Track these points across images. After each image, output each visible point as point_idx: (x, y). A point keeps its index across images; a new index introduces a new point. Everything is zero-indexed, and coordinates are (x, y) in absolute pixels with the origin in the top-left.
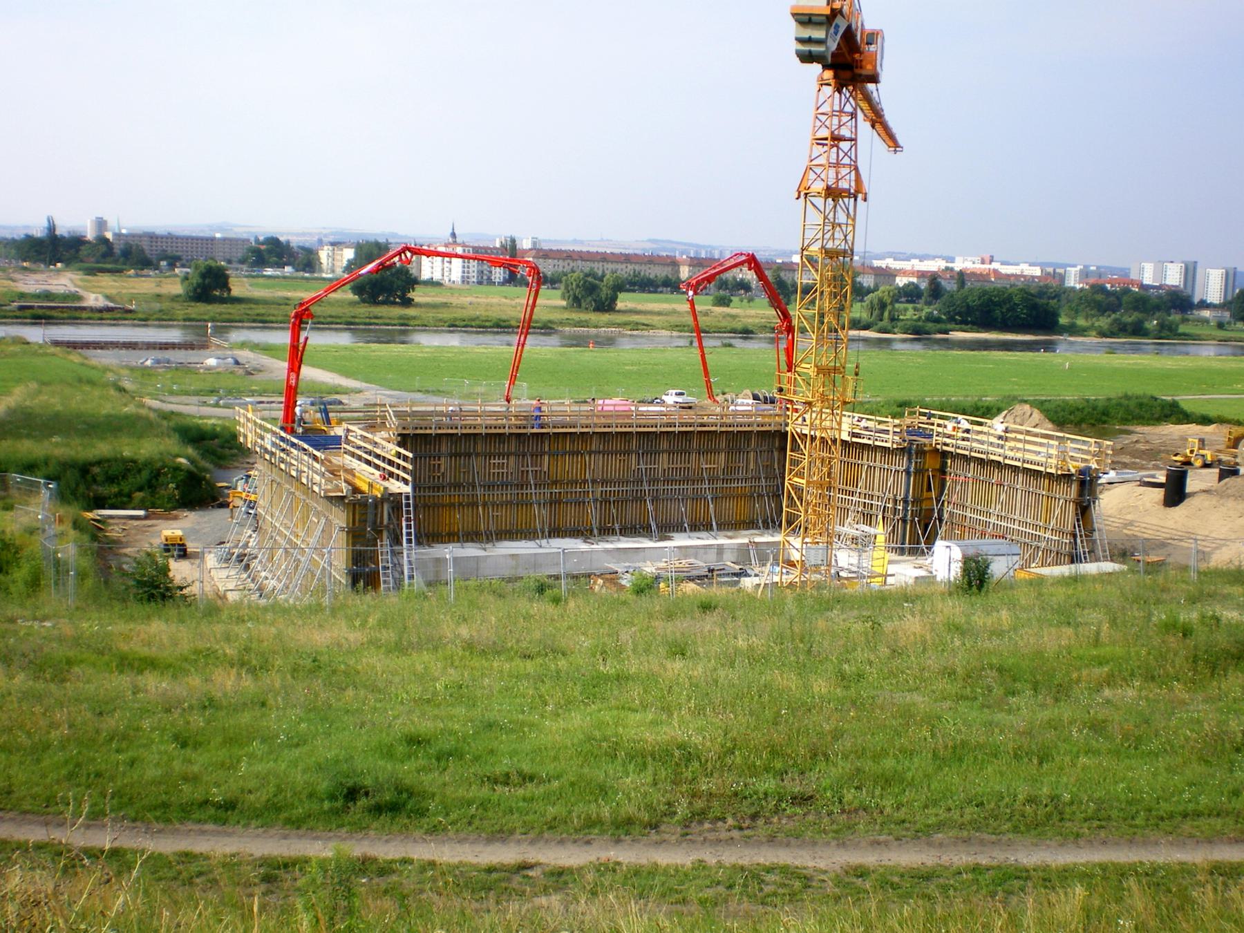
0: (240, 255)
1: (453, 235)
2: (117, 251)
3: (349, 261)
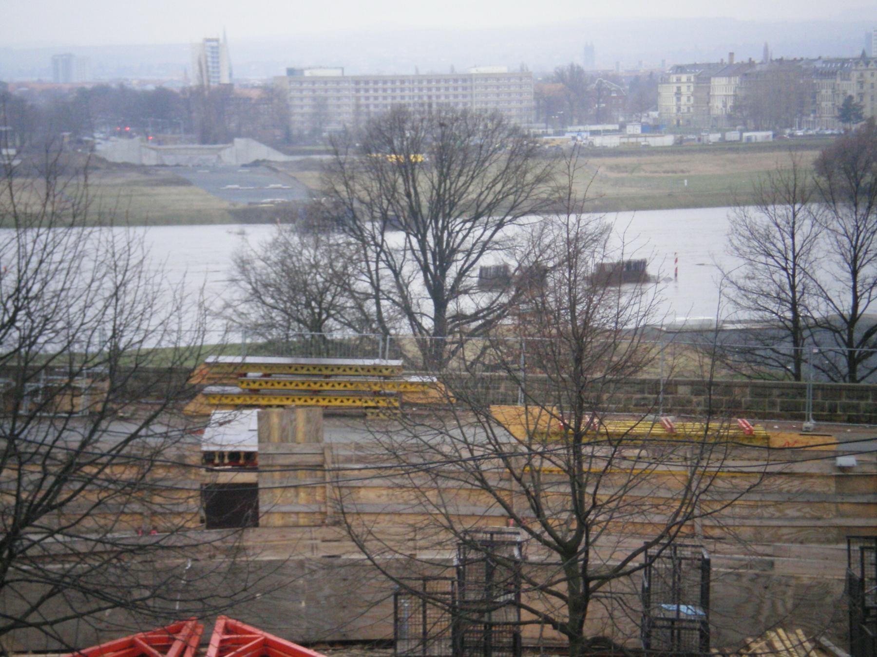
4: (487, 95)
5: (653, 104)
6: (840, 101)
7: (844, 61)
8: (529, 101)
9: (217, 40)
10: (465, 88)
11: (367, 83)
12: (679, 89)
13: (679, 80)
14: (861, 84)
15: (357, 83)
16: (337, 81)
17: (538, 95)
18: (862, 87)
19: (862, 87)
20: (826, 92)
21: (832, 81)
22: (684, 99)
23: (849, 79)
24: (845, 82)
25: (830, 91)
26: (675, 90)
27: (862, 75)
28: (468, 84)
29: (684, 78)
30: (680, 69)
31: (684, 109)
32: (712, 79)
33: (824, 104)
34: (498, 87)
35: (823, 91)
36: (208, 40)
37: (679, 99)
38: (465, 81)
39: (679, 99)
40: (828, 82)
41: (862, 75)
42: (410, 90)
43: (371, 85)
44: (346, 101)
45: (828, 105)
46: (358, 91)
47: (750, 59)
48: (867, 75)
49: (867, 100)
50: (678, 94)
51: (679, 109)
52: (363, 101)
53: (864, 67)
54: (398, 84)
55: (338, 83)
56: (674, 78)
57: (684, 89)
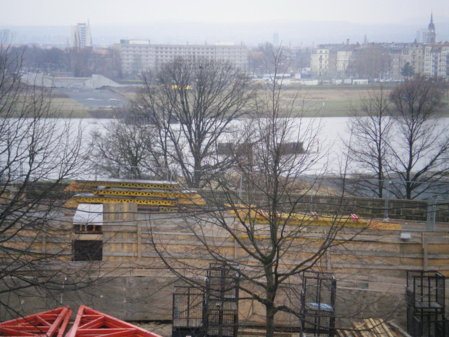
1: (432, 26)
5: (308, 64)
6: (403, 65)
7: (405, 45)
8: (245, 61)
9: (85, 24)
11: (162, 48)
12: (321, 56)
13: (321, 52)
14: (414, 56)
15: (157, 48)
16: (147, 47)
17: (250, 58)
18: (414, 58)
19: (414, 58)
20: (396, 60)
21: (399, 55)
22: (323, 62)
23: (408, 54)
24: (405, 56)
25: (398, 60)
26: (319, 57)
27: (414, 52)
28: (214, 51)
29: (324, 51)
30: (322, 47)
31: (323, 67)
32: (338, 52)
33: (394, 66)
34: (229, 53)
35: (394, 60)
36: (80, 24)
37: (321, 62)
38: (212, 49)
39: (321, 62)
40: (397, 55)
41: (414, 52)
43: (164, 49)
44: (150, 57)
45: (396, 66)
46: (157, 52)
47: (357, 43)
48: (417, 52)
49: (417, 64)
50: (321, 59)
51: (321, 67)
52: (159, 58)
53: (416, 48)
54: (178, 49)
55: (147, 48)
56: (319, 51)
57: (324, 57)
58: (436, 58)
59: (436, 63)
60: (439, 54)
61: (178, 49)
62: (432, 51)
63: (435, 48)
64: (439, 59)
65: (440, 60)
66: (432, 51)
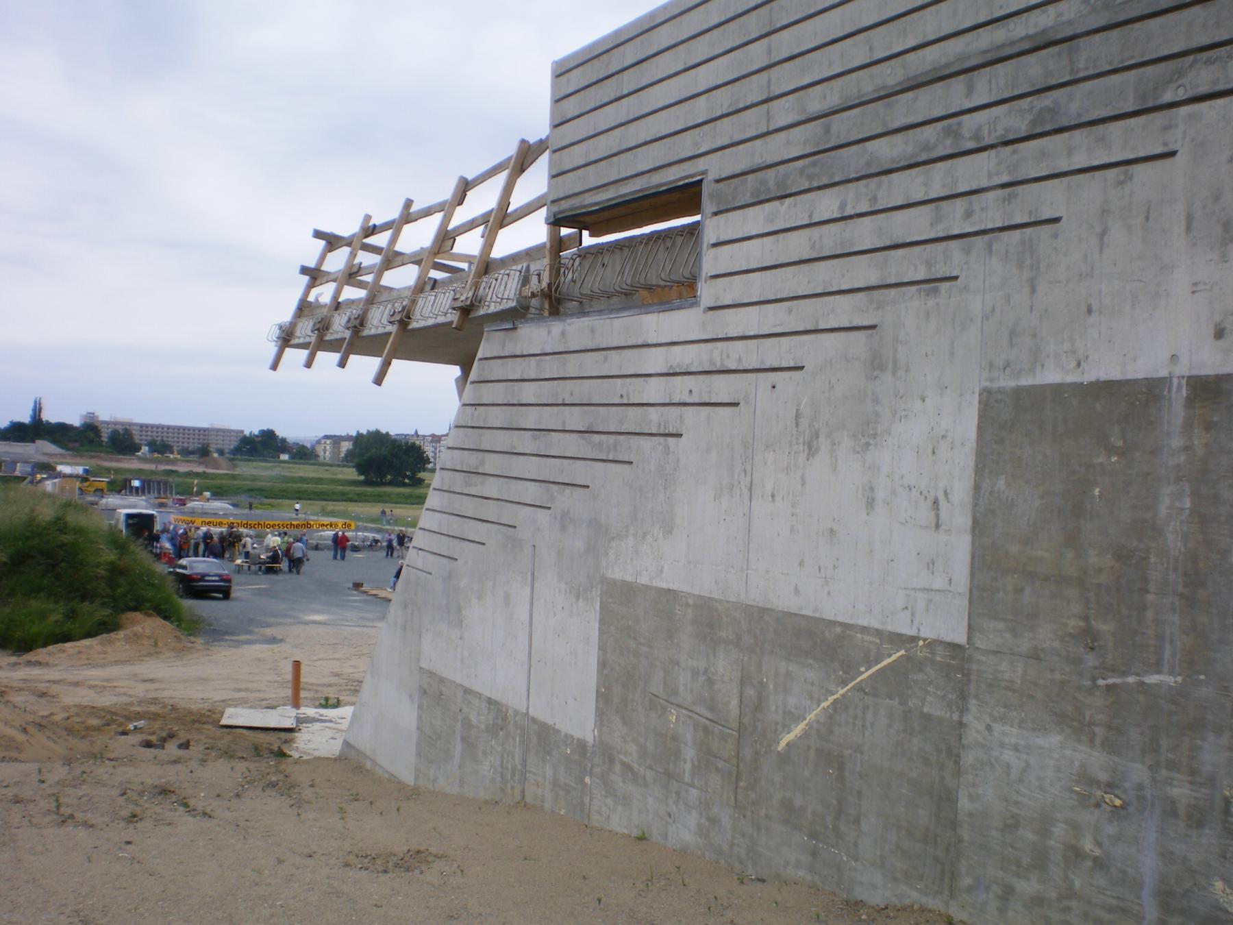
0: (232, 447)
2: (105, 439)
3: (348, 451)
4: (217, 440)
10: (204, 435)
12: (325, 447)
13: (325, 443)
22: (328, 453)
26: (323, 447)
28: (207, 433)
29: (328, 442)
30: (327, 437)
31: (327, 459)
32: (342, 443)
34: (223, 436)
37: (325, 453)
42: (172, 433)
46: (141, 431)
47: (358, 432)
54: (165, 429)
56: (323, 441)
57: (328, 448)
58: (436, 449)
59: (436, 454)
60: (438, 445)
61: (165, 429)
62: (432, 441)
63: (435, 439)
64: (438, 450)
65: (440, 451)
66: (432, 441)
